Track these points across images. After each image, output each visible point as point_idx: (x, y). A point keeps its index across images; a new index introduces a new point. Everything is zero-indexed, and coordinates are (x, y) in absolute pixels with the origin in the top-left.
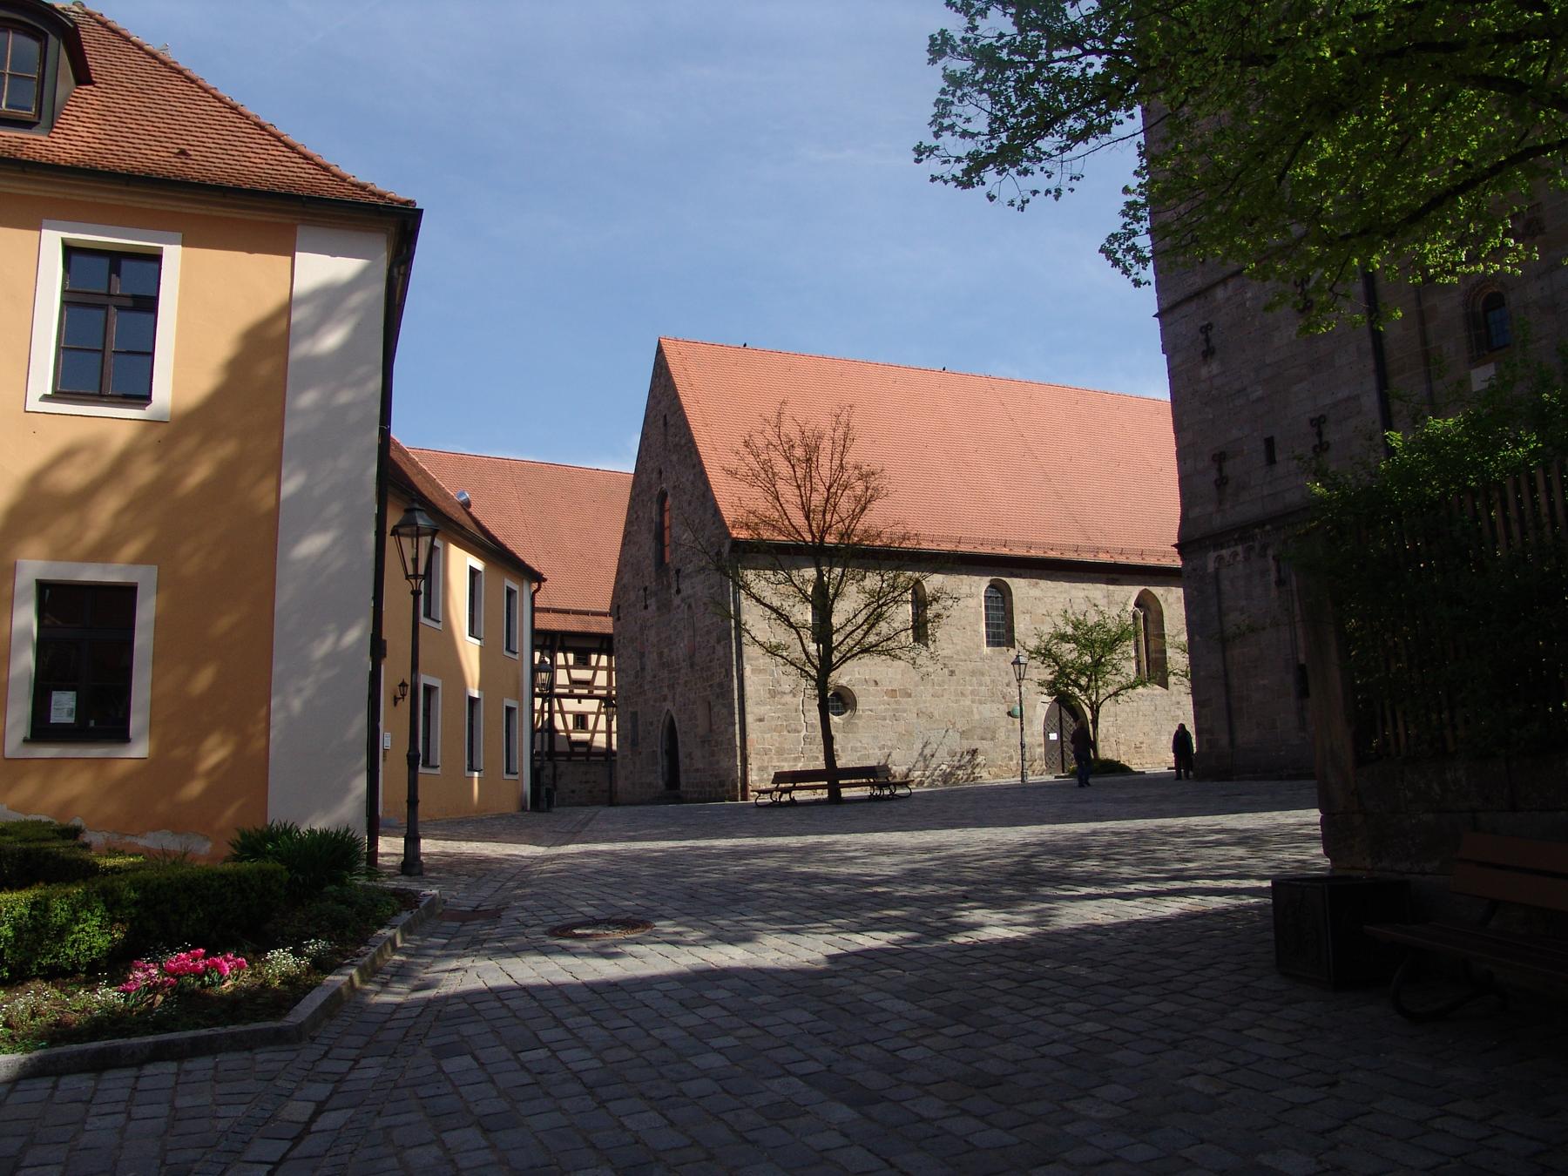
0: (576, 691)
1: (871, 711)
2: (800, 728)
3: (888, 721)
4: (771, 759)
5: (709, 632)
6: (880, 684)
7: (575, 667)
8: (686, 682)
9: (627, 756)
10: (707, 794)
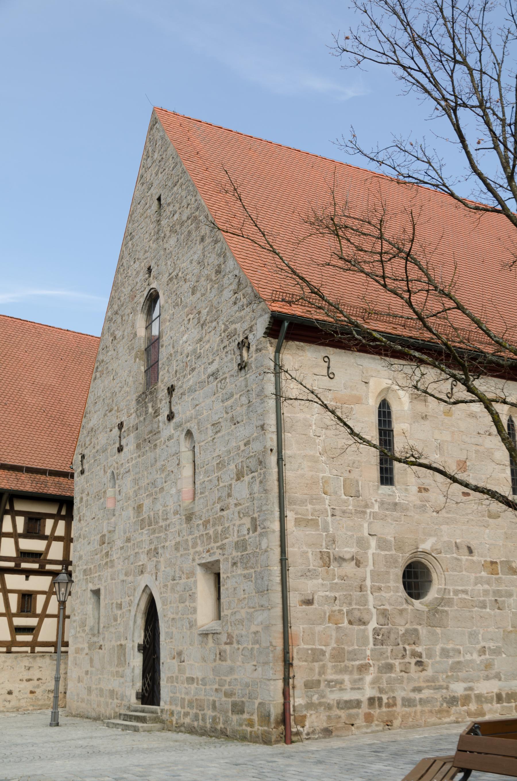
0: (24, 565)
1: (465, 592)
2: (366, 618)
3: (488, 610)
4: (323, 671)
5: (221, 465)
6: (475, 551)
7: (25, 536)
8: (177, 544)
9: (82, 649)
10: (209, 721)
